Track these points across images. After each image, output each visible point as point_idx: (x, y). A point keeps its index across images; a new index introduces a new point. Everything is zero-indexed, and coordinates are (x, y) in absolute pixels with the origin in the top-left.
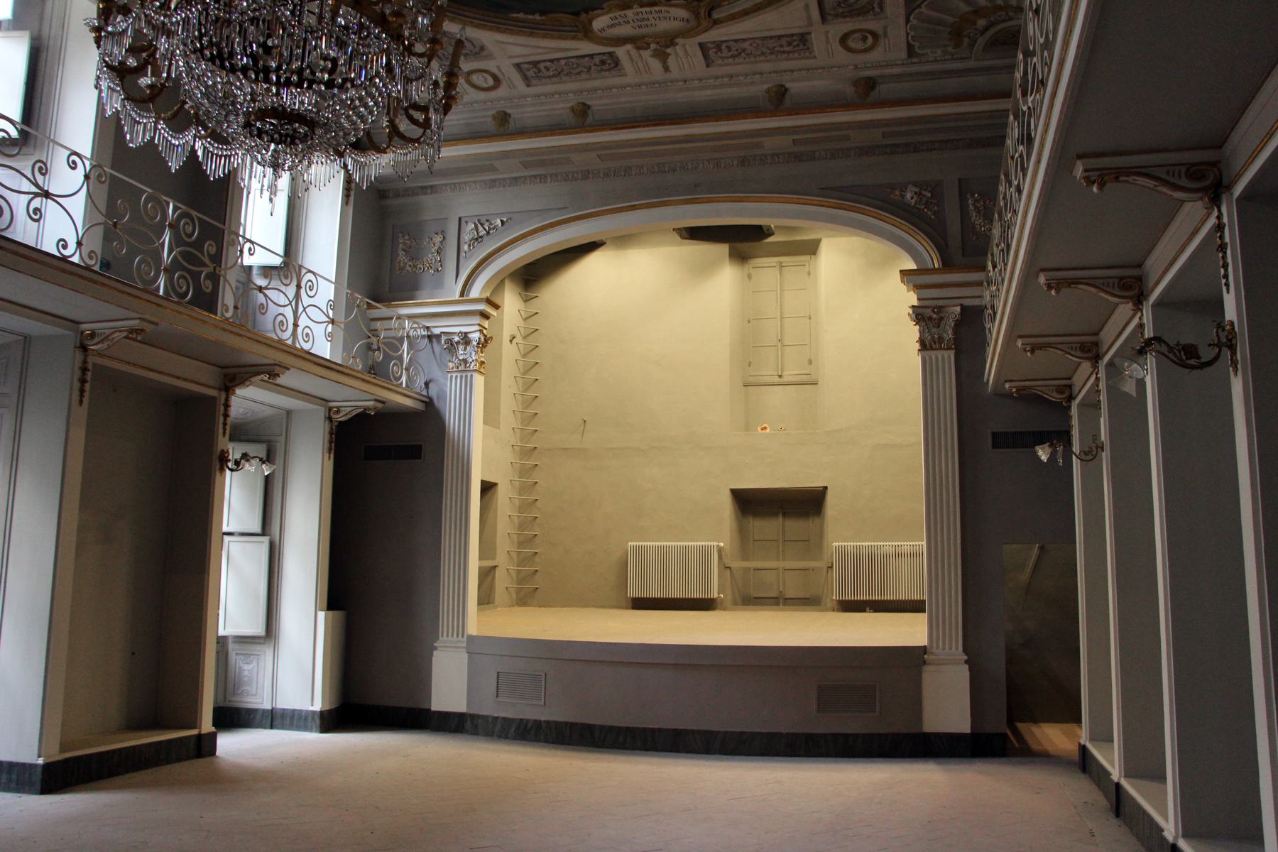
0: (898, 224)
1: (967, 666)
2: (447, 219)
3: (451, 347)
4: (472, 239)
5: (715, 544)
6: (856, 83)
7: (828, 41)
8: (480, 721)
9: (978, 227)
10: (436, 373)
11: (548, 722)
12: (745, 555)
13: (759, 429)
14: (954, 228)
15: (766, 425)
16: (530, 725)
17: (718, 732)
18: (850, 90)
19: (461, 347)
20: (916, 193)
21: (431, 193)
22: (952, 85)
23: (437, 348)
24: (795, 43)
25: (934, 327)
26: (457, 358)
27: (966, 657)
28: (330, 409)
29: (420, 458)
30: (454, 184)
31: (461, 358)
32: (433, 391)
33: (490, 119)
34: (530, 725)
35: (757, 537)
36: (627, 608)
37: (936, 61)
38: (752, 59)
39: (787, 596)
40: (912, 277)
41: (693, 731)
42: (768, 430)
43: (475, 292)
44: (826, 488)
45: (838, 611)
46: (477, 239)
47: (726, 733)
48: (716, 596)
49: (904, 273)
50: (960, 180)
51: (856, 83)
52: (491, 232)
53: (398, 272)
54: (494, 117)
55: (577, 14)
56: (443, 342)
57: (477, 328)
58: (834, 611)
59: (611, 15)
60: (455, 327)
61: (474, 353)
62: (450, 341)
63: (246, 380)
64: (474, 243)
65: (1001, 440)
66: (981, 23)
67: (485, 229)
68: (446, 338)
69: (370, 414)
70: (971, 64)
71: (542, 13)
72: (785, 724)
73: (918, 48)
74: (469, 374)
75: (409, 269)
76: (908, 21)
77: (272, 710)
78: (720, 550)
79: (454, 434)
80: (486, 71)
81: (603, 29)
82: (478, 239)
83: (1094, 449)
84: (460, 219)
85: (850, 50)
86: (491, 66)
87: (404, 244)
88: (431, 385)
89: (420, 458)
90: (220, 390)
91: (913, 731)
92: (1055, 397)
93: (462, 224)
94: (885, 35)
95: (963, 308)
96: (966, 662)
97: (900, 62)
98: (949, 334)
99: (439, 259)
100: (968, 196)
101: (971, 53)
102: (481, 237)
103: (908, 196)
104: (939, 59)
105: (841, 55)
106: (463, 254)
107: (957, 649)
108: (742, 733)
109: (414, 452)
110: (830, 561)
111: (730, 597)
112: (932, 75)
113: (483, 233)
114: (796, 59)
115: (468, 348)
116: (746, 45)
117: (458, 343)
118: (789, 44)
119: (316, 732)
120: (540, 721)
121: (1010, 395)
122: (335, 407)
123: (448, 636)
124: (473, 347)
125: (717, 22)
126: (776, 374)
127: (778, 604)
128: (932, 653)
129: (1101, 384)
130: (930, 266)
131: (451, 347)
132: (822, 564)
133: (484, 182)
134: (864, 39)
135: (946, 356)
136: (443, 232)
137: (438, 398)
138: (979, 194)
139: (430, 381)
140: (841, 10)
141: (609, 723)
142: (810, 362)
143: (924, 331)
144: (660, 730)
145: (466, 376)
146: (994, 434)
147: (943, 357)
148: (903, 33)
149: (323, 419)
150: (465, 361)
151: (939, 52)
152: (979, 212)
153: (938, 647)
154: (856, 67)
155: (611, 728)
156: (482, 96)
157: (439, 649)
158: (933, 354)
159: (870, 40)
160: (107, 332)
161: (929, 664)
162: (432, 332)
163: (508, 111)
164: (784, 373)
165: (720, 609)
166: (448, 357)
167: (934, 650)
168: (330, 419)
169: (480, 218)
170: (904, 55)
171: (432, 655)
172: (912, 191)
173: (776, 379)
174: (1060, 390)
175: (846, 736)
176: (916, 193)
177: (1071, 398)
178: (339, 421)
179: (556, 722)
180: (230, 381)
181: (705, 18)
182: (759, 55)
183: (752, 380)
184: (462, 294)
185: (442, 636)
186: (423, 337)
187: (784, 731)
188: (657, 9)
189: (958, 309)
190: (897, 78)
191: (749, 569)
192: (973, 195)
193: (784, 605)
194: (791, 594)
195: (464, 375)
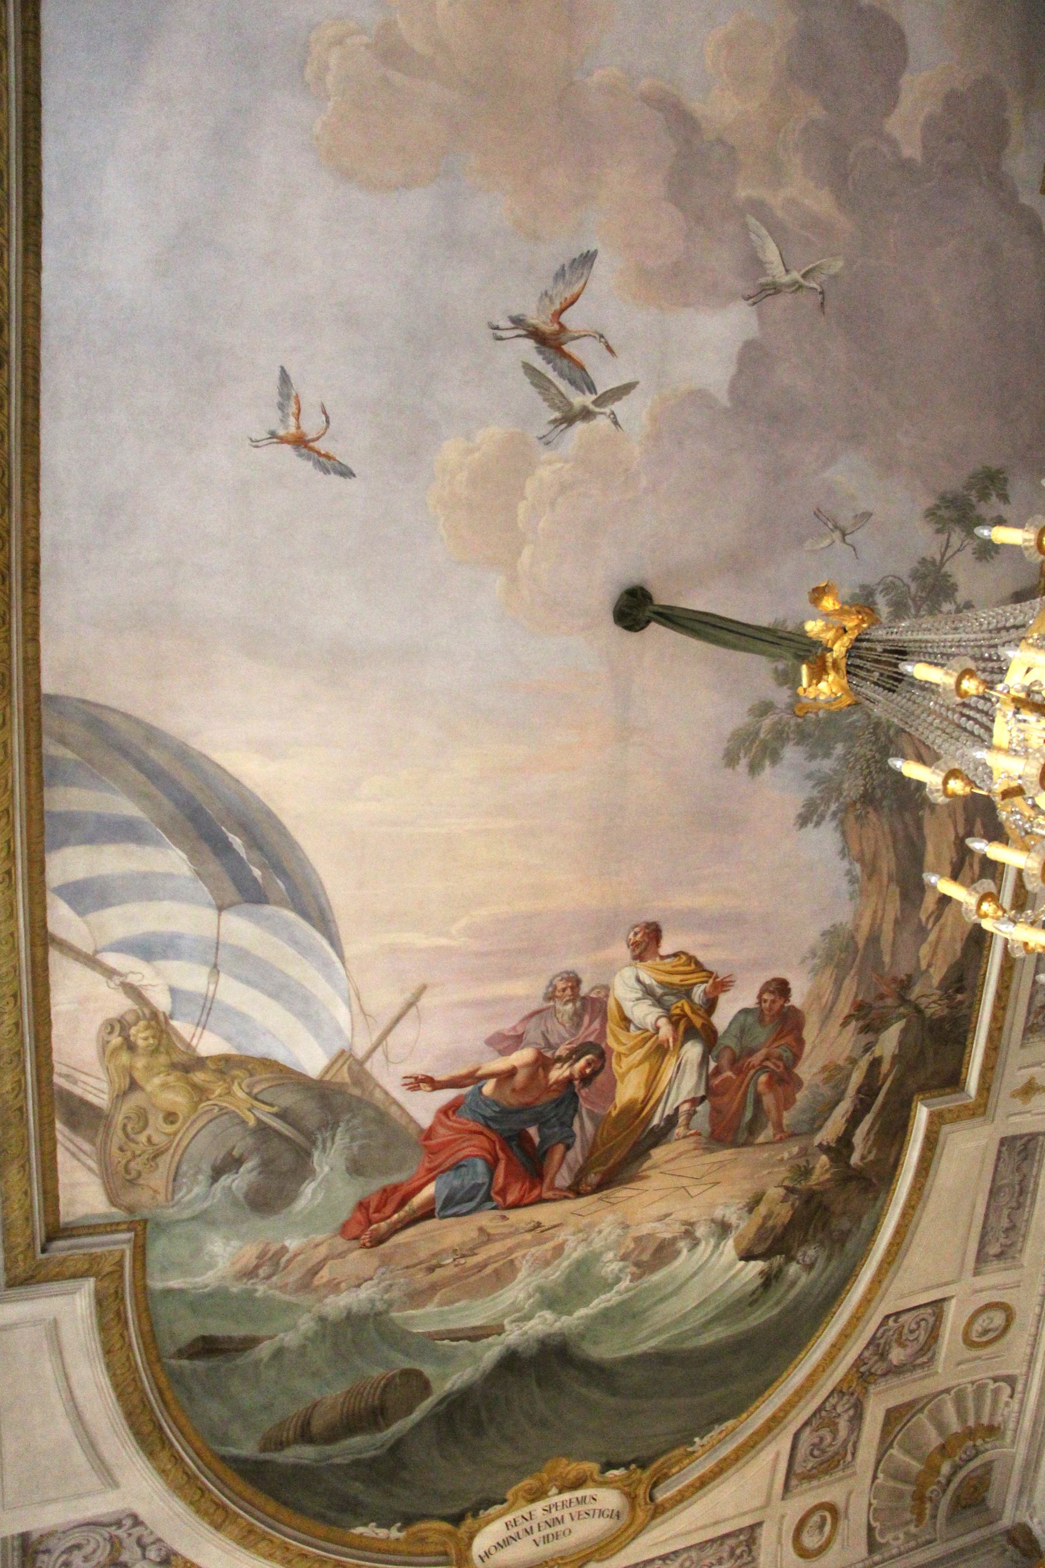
55: (457, 1520)
59: (509, 1518)
66: (946, 1468)
71: (408, 1520)
76: (875, 1477)
81: (488, 1554)
125: (658, 1511)
181: (646, 1504)
188: (579, 1493)
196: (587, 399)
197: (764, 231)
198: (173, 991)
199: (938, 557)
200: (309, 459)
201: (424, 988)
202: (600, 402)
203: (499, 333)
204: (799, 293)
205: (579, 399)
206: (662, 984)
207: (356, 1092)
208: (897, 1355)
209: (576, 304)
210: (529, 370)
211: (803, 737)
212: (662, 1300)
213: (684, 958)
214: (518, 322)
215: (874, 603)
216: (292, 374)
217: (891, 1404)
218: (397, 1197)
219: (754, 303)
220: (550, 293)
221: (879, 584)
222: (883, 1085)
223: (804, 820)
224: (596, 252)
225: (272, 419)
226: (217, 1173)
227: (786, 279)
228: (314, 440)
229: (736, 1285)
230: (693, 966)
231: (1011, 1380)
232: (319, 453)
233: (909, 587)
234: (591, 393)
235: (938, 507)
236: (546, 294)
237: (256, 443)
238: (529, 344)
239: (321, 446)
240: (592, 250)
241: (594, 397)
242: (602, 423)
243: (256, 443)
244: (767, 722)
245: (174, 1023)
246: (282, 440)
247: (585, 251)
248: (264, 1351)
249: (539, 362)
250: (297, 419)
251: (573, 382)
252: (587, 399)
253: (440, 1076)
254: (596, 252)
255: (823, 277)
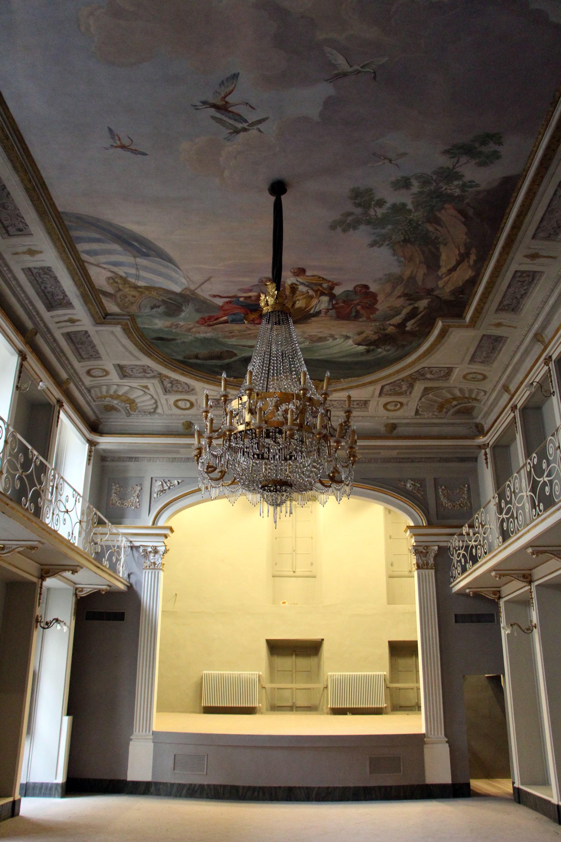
0: (403, 500)
1: (447, 745)
2: (143, 477)
3: (146, 555)
4: (160, 491)
5: (257, 673)
6: (386, 426)
7: (377, 405)
8: (161, 786)
9: (444, 504)
10: (135, 569)
11: (209, 786)
12: (272, 680)
13: (281, 603)
14: (432, 502)
15: (285, 601)
16: (196, 789)
17: (314, 788)
18: (382, 429)
19: (152, 555)
20: (412, 484)
21: (135, 461)
22: (435, 430)
23: (136, 554)
24: (360, 404)
25: (424, 557)
26: (149, 561)
27: (447, 739)
28: (76, 589)
29: (123, 620)
30: (150, 457)
31: (152, 561)
32: (133, 580)
33: (180, 425)
34: (196, 789)
35: (279, 669)
36: (200, 713)
37: (428, 418)
38: (336, 409)
39: (298, 706)
40: (412, 530)
41: (299, 788)
42: (287, 604)
43: (161, 523)
44: (323, 640)
45: (331, 714)
46: (162, 491)
47: (319, 787)
48: (257, 705)
49: (409, 527)
50: (435, 479)
51: (386, 426)
52: (171, 488)
53: (112, 506)
54: (183, 424)
56: (141, 551)
57: (163, 544)
58: (328, 714)
60: (150, 543)
61: (160, 559)
62: (145, 551)
63: (57, 573)
64: (160, 493)
65: (459, 619)
66: (455, 403)
67: (167, 485)
68: (143, 549)
69: (102, 593)
70: (445, 421)
71: (235, 378)
72: (352, 782)
73: (421, 411)
74: (157, 572)
75: (119, 505)
76: (420, 399)
77: (27, 783)
78: (259, 676)
79: (146, 607)
80: (188, 400)
82: (163, 491)
83: (532, 628)
84: (152, 478)
85: (388, 410)
86: (192, 398)
87: (116, 489)
88: (131, 576)
89: (123, 620)
90: (39, 578)
91: (415, 782)
92: (491, 597)
93: (153, 482)
94: (407, 404)
95: (438, 546)
96: (447, 742)
97: (411, 417)
98: (431, 561)
99: (138, 500)
100: (439, 487)
101: (446, 416)
102: (165, 490)
103: (408, 485)
104: (430, 417)
105: (382, 412)
106: (153, 499)
107: (441, 734)
108: (328, 788)
109: (120, 617)
110: (326, 684)
111: (265, 707)
112: (426, 425)
113: (166, 488)
114: (358, 411)
115: (156, 556)
116: (334, 403)
117: (150, 552)
118: (358, 404)
119: (58, 797)
120: (204, 785)
121: (467, 595)
122: (80, 588)
123: (139, 732)
124: (160, 555)
126: (292, 570)
127: (292, 710)
128: (428, 738)
129: (533, 593)
130: (421, 524)
131: (146, 555)
132: (321, 686)
133: (169, 458)
134: (396, 405)
135: (430, 573)
136: (141, 485)
137: (136, 583)
138: (445, 487)
139: (131, 574)
140: (390, 392)
141: (247, 784)
142: (312, 564)
143: (418, 559)
144: (280, 787)
145: (155, 573)
146: (456, 616)
147: (429, 573)
148: (416, 404)
149: (72, 595)
150: (155, 563)
151: (431, 414)
152: (444, 496)
153: (431, 734)
154: (388, 418)
155: (249, 787)
156: (179, 412)
157: (133, 740)
158: (423, 571)
159: (399, 406)
160: (14, 547)
161: (427, 744)
162: (133, 544)
163: (192, 422)
164: (297, 570)
165: (259, 713)
166: (143, 560)
167: (429, 735)
168: (76, 595)
169: (164, 479)
170: (413, 413)
171: (128, 744)
172: (410, 483)
173: (292, 574)
174: (494, 593)
175: (386, 787)
176: (412, 484)
177: (500, 598)
178: (81, 597)
179: (214, 785)
180: (46, 573)
182: (340, 408)
183: (277, 573)
184: (153, 524)
185: (136, 732)
186: (129, 546)
187: (351, 785)
189: (436, 548)
190: (408, 425)
191: (275, 688)
192: (441, 487)
193: (296, 711)
194: (299, 703)
195: (154, 571)
196: (245, 125)
197: (335, 52)
198: (125, 273)
199: (451, 167)
200: (129, 151)
201: (211, 277)
202: (253, 124)
203: (197, 107)
204: (360, 74)
205: (240, 126)
206: (307, 282)
207: (194, 296)
208: (429, 376)
209: (232, 94)
210: (213, 118)
211: (369, 223)
212: (322, 349)
213: (317, 277)
214: (204, 103)
215: (410, 182)
216: (113, 128)
217: (426, 386)
218: (215, 318)
219: (331, 82)
220: (218, 91)
221: (413, 176)
222: (420, 314)
223: (372, 245)
224: (238, 73)
225: (111, 142)
226: (152, 308)
227: (350, 70)
228: (128, 146)
229: (355, 350)
230: (321, 279)
231: (485, 392)
232: (132, 150)
233: (432, 177)
234: (246, 123)
235: (452, 149)
236: (216, 92)
237: (107, 149)
238: (213, 110)
239: (133, 147)
240: (236, 72)
241: (247, 124)
242: (253, 132)
243: (107, 149)
244: (350, 219)
245: (129, 279)
246: (116, 147)
247: (233, 74)
248: (179, 341)
249: (218, 115)
250: (120, 140)
251: (235, 120)
252: (245, 125)
253: (222, 295)
254: (238, 73)
255: (375, 66)
